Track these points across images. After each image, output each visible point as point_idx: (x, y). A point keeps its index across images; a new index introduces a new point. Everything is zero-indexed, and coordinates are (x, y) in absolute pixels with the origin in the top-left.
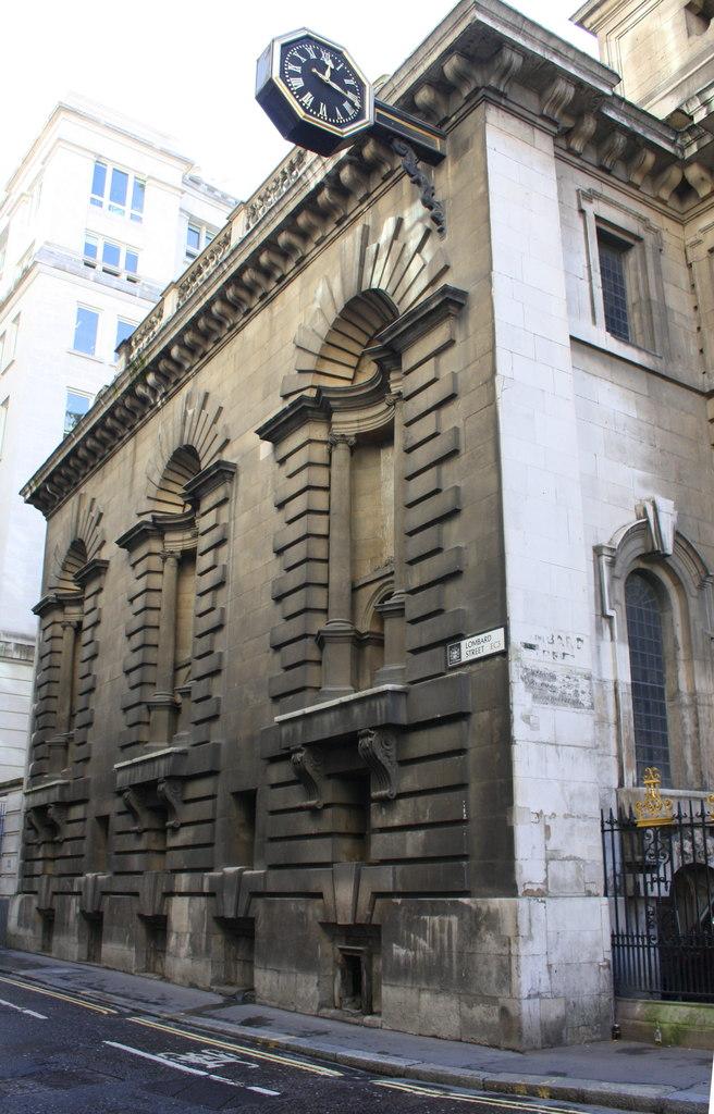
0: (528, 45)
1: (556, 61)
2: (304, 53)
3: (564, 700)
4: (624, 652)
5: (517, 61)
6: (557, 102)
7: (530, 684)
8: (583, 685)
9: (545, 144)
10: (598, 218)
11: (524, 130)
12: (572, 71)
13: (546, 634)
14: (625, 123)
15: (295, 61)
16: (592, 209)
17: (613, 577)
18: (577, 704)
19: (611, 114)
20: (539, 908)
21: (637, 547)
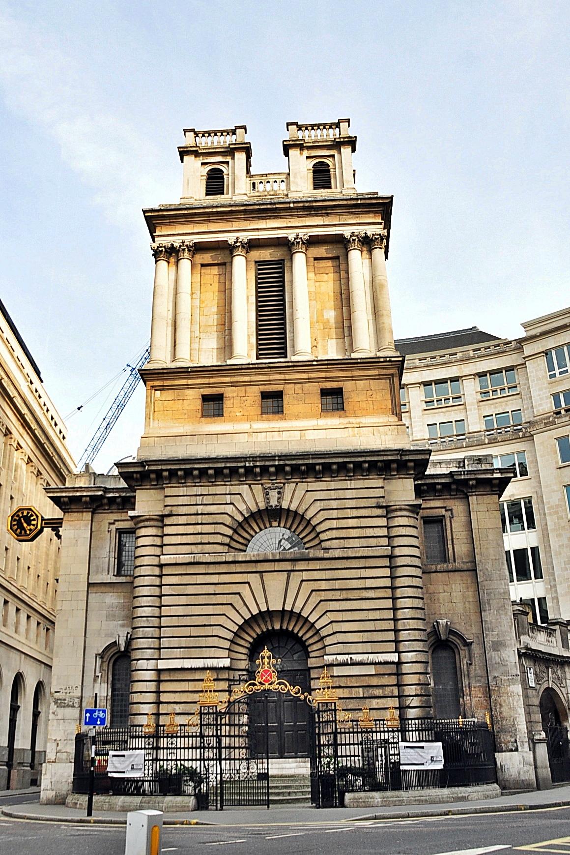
0: (67, 494)
1: (78, 494)
2: (18, 516)
3: (68, 706)
4: (104, 685)
5: (66, 499)
6: (86, 502)
7: (56, 703)
8: (77, 700)
9: (88, 516)
10: (117, 529)
11: (80, 515)
12: (85, 494)
13: (64, 687)
14: (117, 495)
15: (15, 520)
16: (113, 528)
17: (102, 662)
18: (73, 706)
19: (111, 495)
20: (49, 766)
21: (113, 650)
